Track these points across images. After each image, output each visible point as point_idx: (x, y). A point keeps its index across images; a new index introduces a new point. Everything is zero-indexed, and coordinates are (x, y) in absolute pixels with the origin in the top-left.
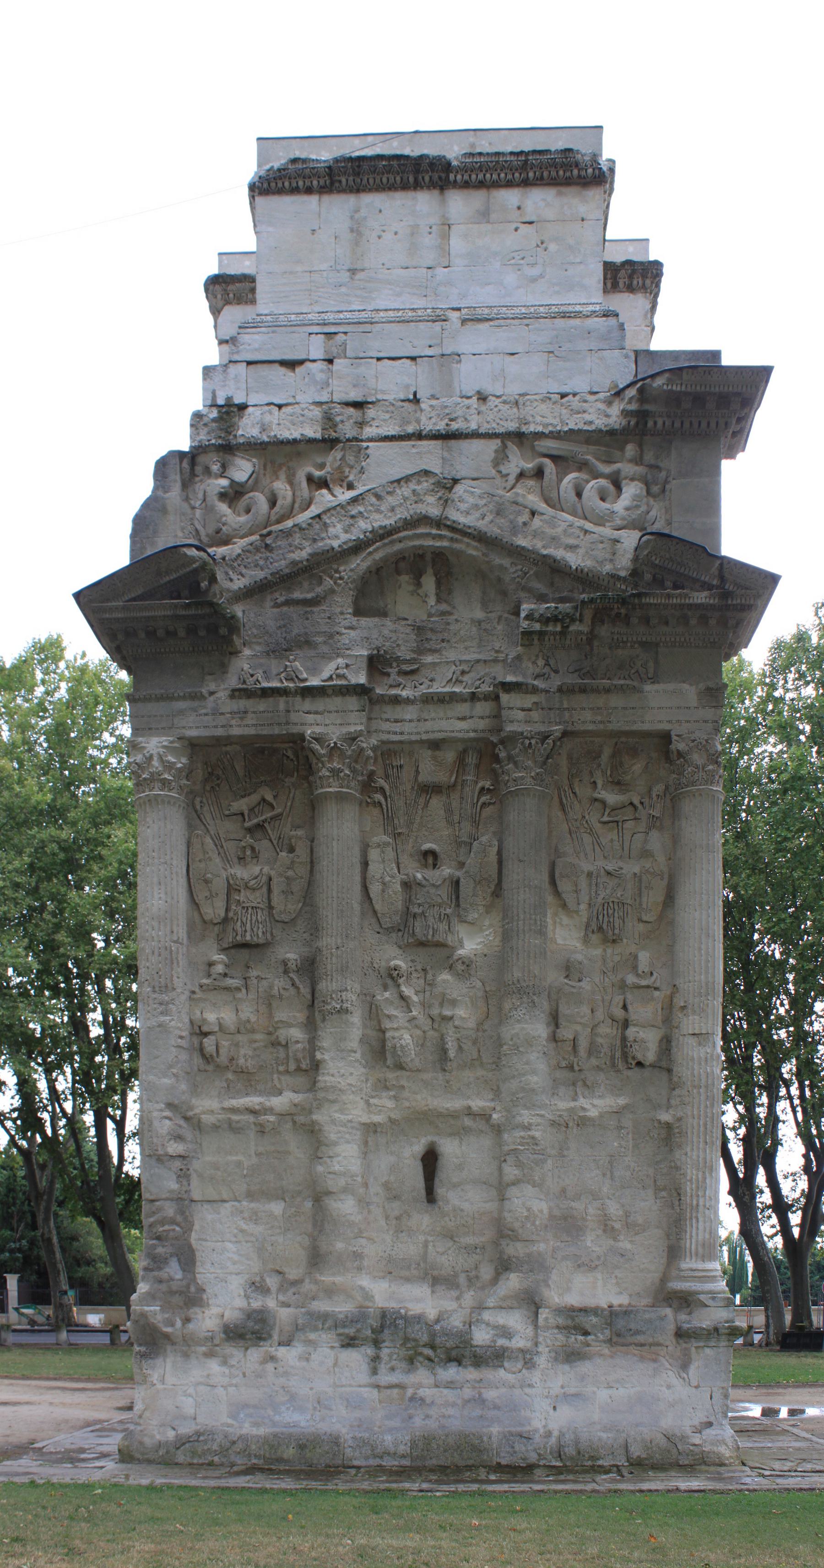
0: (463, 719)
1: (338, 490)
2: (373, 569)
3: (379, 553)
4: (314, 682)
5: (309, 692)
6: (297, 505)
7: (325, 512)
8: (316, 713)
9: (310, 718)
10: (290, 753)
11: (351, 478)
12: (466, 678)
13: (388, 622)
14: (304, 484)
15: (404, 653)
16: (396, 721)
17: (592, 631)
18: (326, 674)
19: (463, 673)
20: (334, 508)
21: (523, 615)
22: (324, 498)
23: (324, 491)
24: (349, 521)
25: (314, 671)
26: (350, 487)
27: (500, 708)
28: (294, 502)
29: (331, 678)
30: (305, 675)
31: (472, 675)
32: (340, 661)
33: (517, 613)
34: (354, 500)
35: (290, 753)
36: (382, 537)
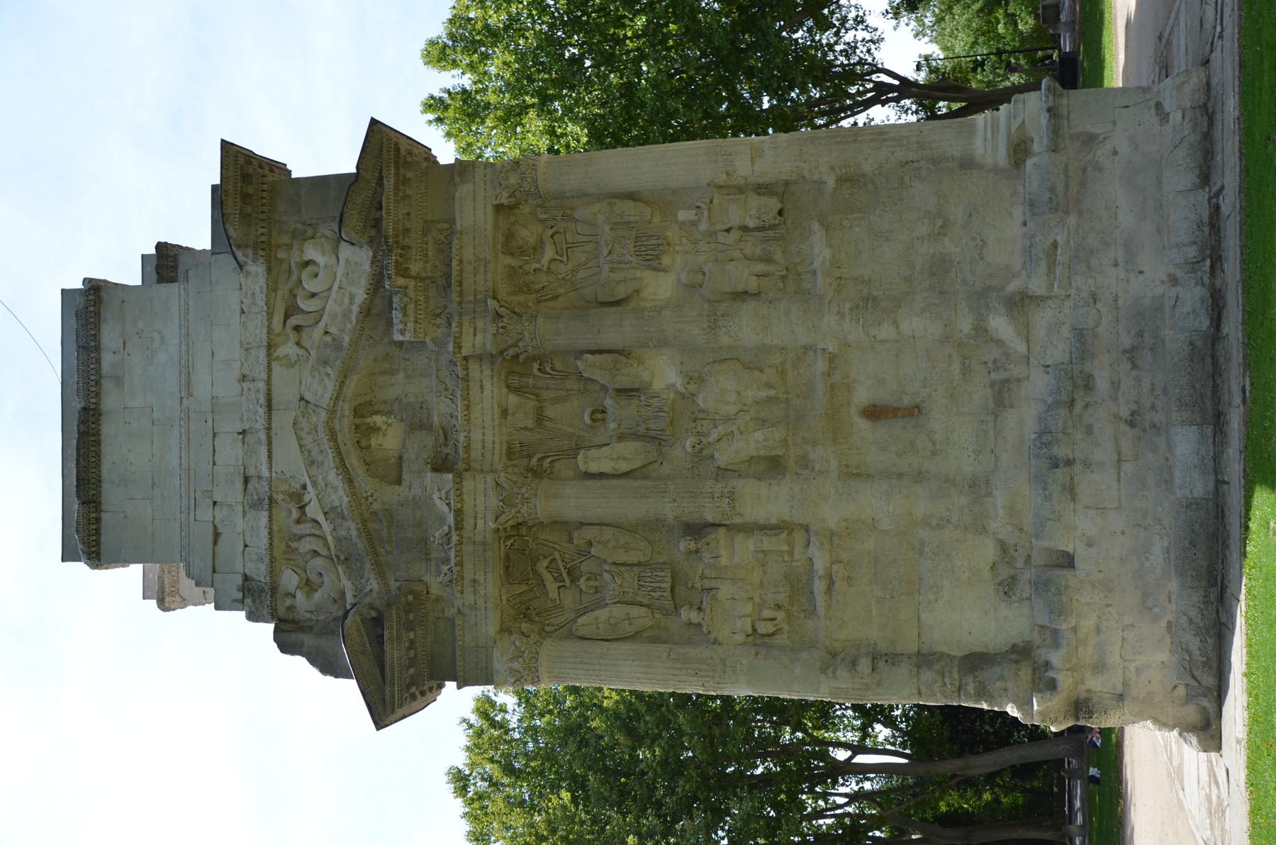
0: (482, 387)
1: (306, 498)
2: (365, 468)
3: (353, 461)
4: (451, 519)
5: (459, 526)
6: (317, 533)
7: (323, 509)
8: (476, 518)
9: (480, 523)
10: (509, 543)
11: (298, 486)
12: (450, 386)
13: (406, 456)
14: (301, 526)
15: (429, 441)
16: (484, 447)
17: (415, 278)
18: (446, 509)
19: (446, 389)
20: (319, 500)
21: (401, 338)
22: (313, 510)
23: (307, 509)
24: (329, 489)
25: (442, 519)
26: (304, 487)
27: (472, 356)
28: (314, 535)
29: (448, 504)
30: (446, 528)
31: (447, 381)
32: (435, 496)
33: (401, 344)
34: (314, 484)
35: (509, 543)
36: (342, 460)
